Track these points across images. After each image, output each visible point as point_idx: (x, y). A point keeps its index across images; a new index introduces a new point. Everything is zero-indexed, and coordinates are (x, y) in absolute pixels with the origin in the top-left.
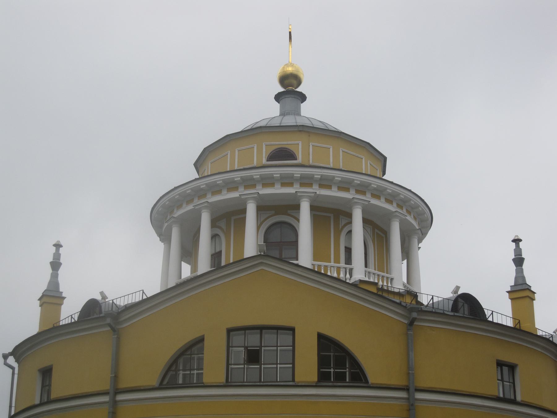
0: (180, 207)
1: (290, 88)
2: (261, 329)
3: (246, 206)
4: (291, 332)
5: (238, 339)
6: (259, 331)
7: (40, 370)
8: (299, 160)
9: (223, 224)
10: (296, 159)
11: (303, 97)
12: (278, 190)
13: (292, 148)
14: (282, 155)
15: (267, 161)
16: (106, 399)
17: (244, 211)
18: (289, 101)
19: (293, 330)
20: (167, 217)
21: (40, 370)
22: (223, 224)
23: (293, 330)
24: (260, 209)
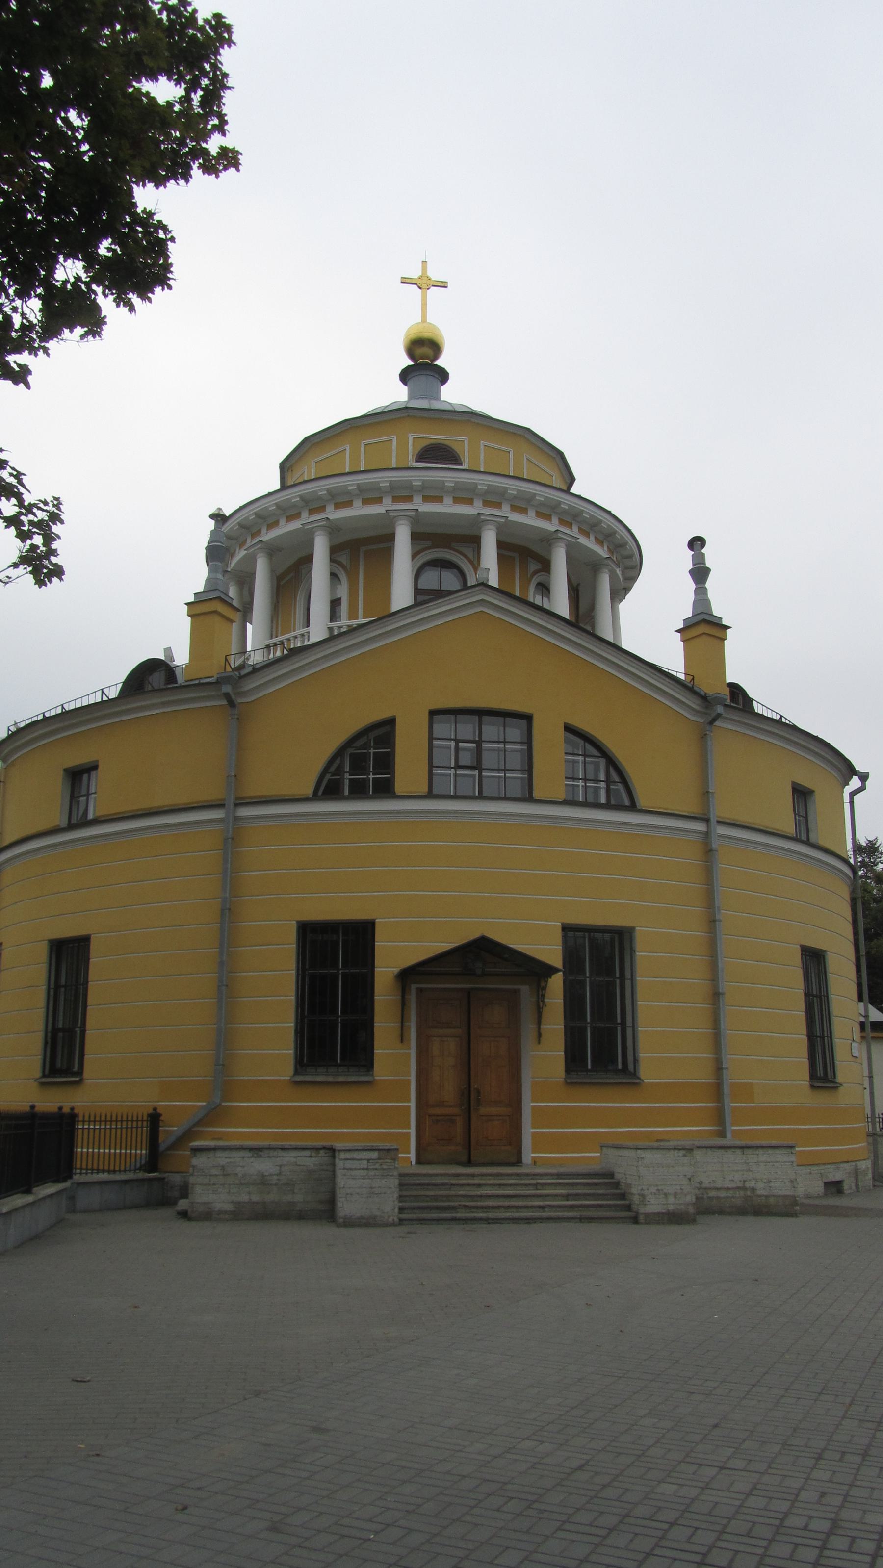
0: (271, 526)
1: (424, 360)
3: (394, 528)
4: (524, 723)
5: (443, 728)
6: (476, 718)
7: (66, 770)
8: (465, 466)
9: (344, 559)
10: (461, 464)
11: (443, 376)
12: (448, 507)
13: (456, 447)
14: (438, 454)
15: (417, 461)
17: (390, 538)
18: (422, 381)
19: (528, 718)
20: (245, 541)
21: (66, 770)
22: (344, 559)
23: (528, 718)
24: (416, 537)
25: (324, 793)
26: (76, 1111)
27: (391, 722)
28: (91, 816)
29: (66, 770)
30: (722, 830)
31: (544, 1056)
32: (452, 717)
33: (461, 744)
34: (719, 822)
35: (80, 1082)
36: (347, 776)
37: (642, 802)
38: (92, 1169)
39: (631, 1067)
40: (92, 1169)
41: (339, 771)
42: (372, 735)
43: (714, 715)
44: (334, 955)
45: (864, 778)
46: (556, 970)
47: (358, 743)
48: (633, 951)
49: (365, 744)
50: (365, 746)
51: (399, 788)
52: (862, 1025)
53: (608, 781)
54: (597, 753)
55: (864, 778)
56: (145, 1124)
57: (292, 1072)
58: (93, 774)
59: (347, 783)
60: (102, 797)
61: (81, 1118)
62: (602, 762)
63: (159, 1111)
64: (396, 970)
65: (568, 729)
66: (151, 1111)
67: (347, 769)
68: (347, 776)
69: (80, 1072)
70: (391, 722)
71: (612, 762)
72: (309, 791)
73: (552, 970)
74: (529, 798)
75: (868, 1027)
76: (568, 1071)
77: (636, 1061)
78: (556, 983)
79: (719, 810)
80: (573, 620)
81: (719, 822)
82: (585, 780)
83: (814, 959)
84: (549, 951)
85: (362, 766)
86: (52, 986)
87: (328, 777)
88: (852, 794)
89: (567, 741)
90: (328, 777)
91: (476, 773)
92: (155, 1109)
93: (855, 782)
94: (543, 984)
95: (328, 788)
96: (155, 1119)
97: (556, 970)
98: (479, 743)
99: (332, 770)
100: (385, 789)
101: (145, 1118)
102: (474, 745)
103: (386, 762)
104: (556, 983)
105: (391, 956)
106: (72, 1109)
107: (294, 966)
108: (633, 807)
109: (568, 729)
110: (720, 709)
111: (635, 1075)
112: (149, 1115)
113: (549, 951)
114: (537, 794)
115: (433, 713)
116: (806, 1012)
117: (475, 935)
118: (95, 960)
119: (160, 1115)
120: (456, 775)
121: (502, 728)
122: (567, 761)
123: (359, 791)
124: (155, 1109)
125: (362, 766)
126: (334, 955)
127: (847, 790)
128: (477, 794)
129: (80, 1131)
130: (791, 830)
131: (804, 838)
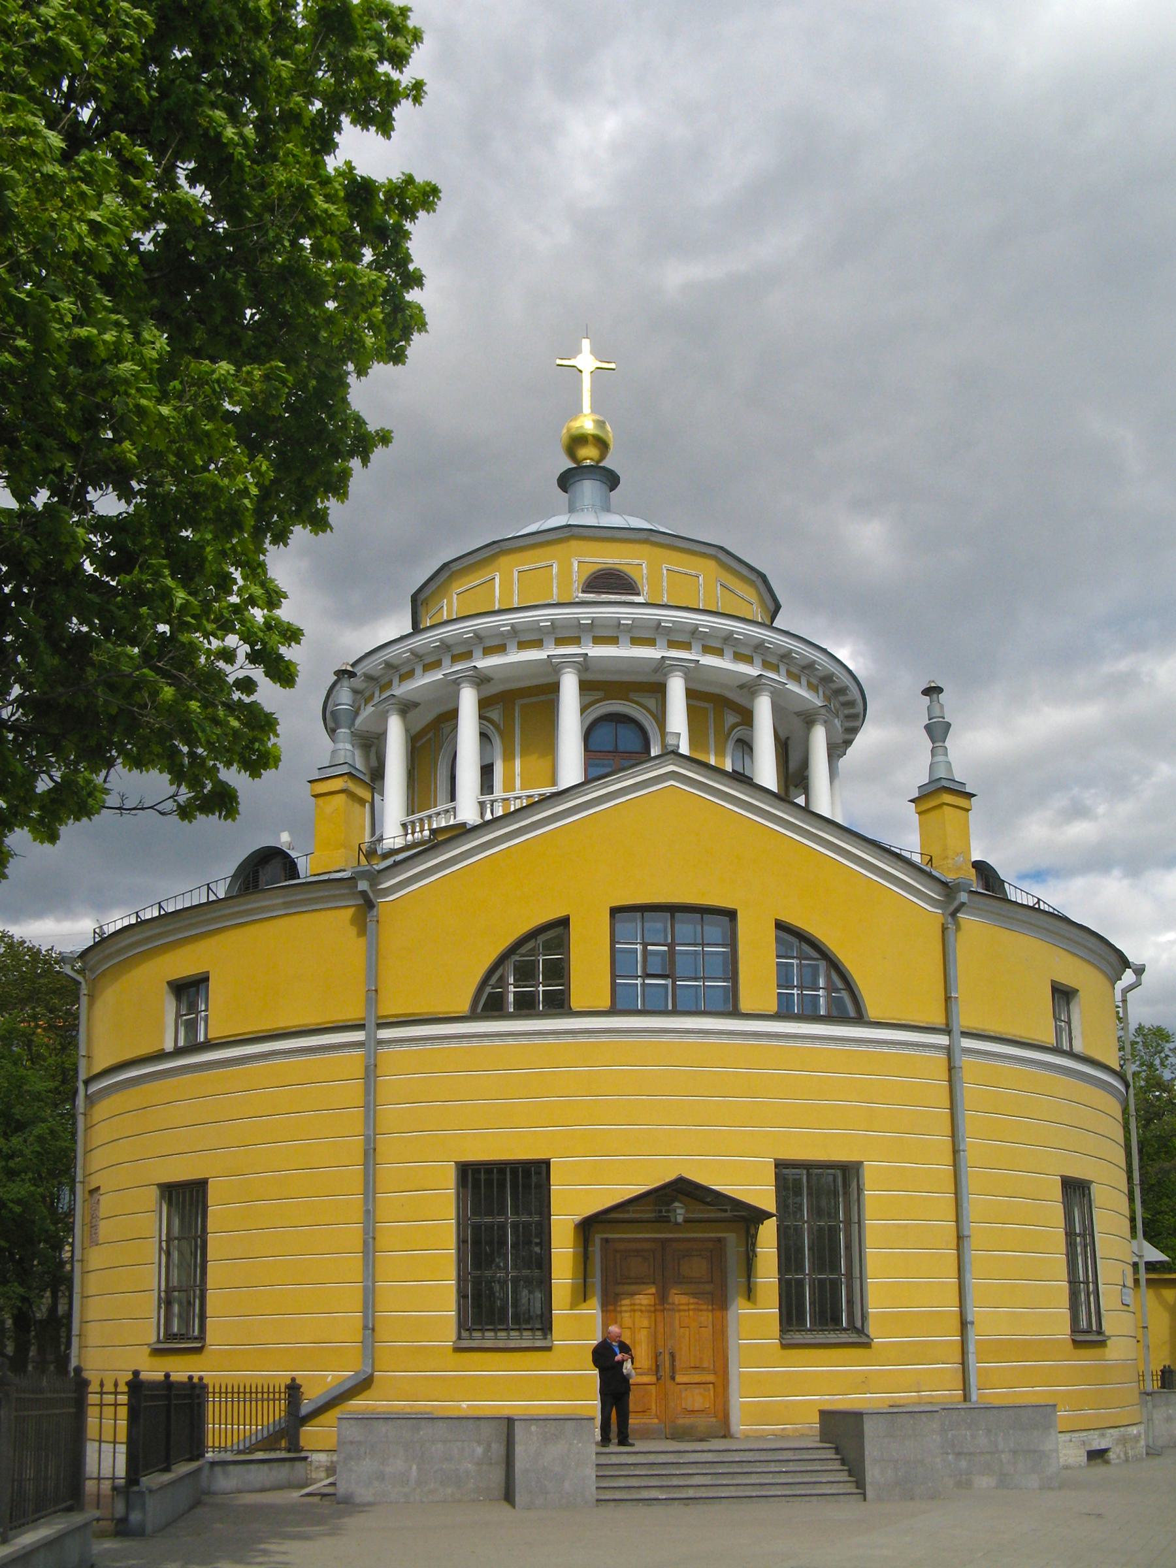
2: (673, 910)
16: (359, 1036)
19: (732, 915)
23: (732, 915)
25: (485, 1008)
26: (205, 1381)
27: (564, 922)
28: (201, 1038)
29: (169, 983)
30: (967, 1043)
31: (756, 1317)
32: (639, 915)
33: (649, 948)
34: (965, 1034)
35: (202, 1348)
36: (512, 988)
37: (872, 1013)
38: (220, 1447)
39: (858, 1324)
40: (220, 1447)
41: (502, 981)
42: (541, 939)
43: (956, 904)
44: (502, 1200)
45: (1140, 971)
46: (769, 1215)
47: (523, 950)
48: (860, 1190)
49: (533, 949)
50: (532, 952)
51: (575, 1005)
52: (1135, 1265)
53: (831, 988)
54: (816, 955)
55: (1140, 971)
56: (283, 1396)
57: (454, 1337)
58: (202, 986)
59: (511, 998)
60: (219, 1016)
61: (211, 1390)
62: (822, 965)
63: (298, 1381)
64: (578, 1218)
65: (780, 926)
66: (289, 1382)
67: (511, 980)
68: (512, 988)
69: (202, 1337)
70: (564, 922)
71: (834, 965)
72: (464, 1007)
73: (764, 1215)
74: (735, 1012)
75: (1142, 1268)
76: (783, 1331)
77: (864, 1317)
78: (768, 1233)
79: (966, 1019)
80: (783, 794)
81: (962, 1033)
82: (801, 987)
83: (1075, 1191)
84: (763, 1195)
85: (529, 977)
86: (164, 1238)
87: (488, 990)
88: (1126, 991)
89: (778, 940)
90: (488, 990)
91: (669, 982)
92: (293, 1379)
93: (1128, 977)
94: (752, 1231)
95: (489, 1004)
96: (293, 1389)
97: (769, 1215)
98: (671, 946)
99: (493, 981)
100: (558, 1004)
101: (283, 1390)
102: (665, 948)
103: (559, 971)
104: (768, 1233)
105: (571, 1202)
106: (201, 1378)
107: (453, 1214)
108: (860, 1019)
109: (780, 926)
110: (963, 897)
111: (861, 1331)
112: (288, 1387)
113: (763, 1195)
114: (745, 1006)
115: (615, 911)
116: (1067, 1255)
117: (670, 1177)
118: (214, 1210)
119: (299, 1387)
120: (643, 985)
121: (699, 928)
122: (778, 964)
123: (526, 1006)
124: (293, 1379)
125: (529, 977)
126: (502, 1200)
127: (1120, 985)
128: (670, 1008)
129: (211, 1404)
130: (1050, 1039)
131: (1066, 1047)
